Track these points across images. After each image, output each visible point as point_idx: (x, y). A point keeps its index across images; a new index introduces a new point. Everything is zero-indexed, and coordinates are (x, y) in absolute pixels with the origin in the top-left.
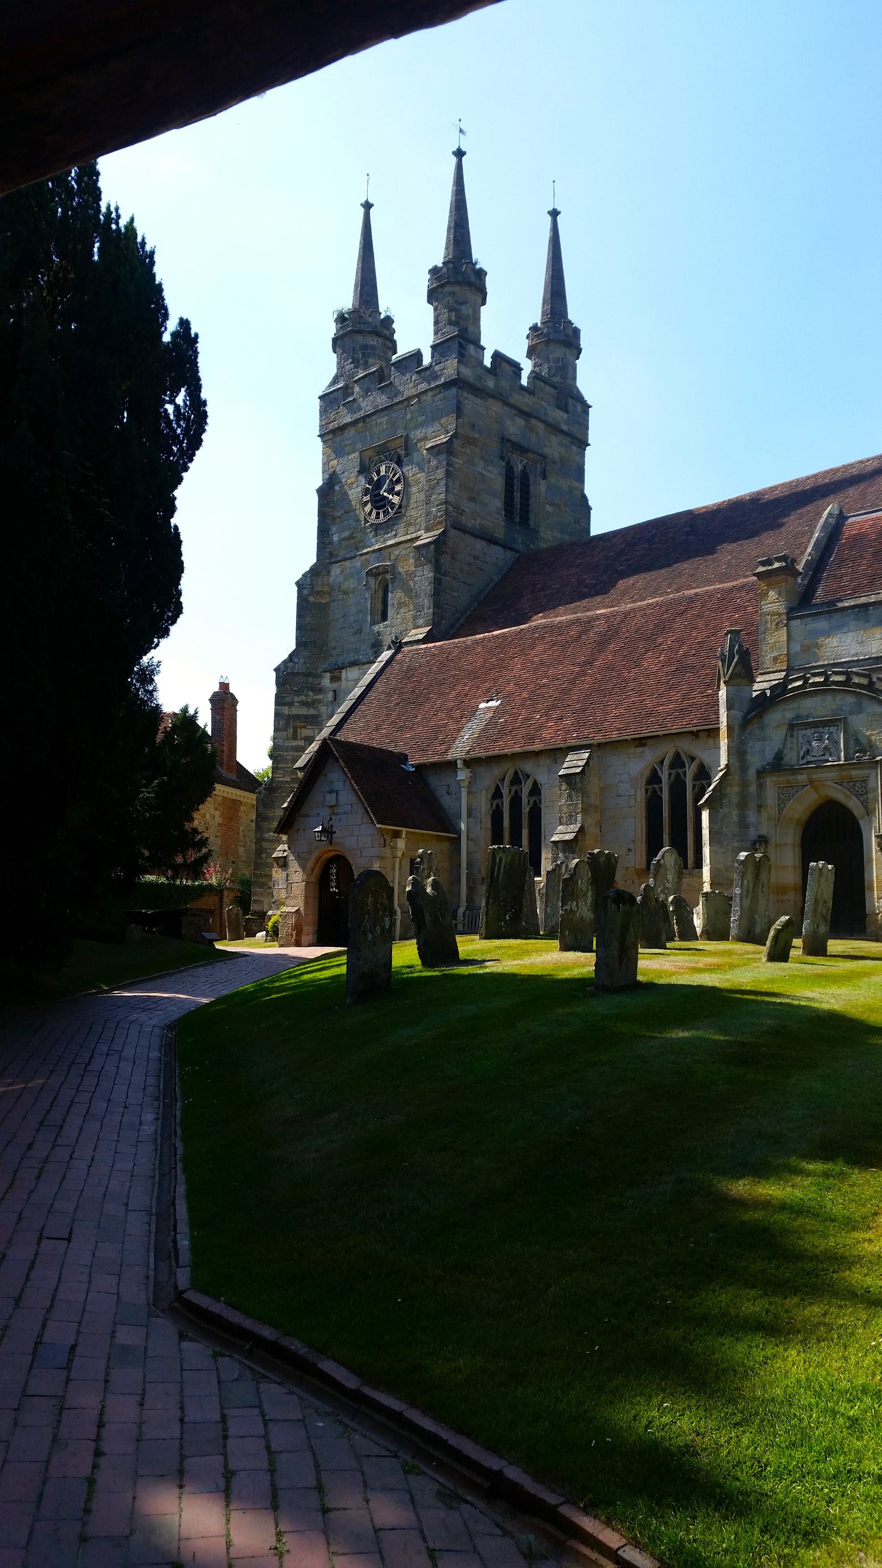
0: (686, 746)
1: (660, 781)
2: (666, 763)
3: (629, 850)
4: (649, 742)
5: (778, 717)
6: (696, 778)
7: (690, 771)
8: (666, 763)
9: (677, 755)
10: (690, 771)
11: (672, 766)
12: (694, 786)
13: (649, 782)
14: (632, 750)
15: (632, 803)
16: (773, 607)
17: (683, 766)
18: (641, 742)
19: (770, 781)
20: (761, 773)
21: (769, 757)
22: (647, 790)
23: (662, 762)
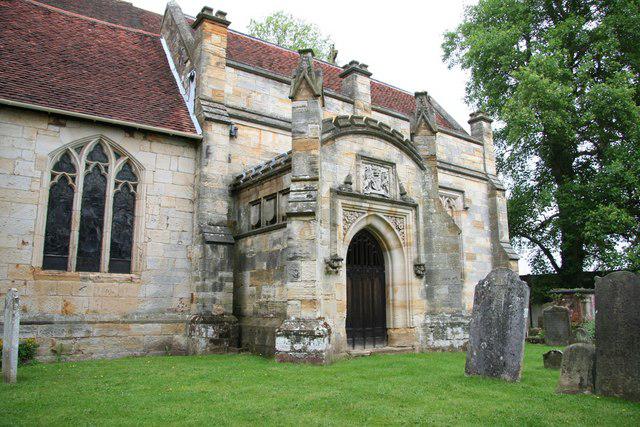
0: (119, 139)
1: (73, 168)
2: (86, 151)
3: (23, 243)
4: (69, 124)
5: (349, 145)
6: (120, 175)
7: (114, 167)
8: (86, 151)
9: (99, 146)
10: (114, 167)
11: (91, 156)
12: (117, 184)
13: (57, 167)
14: (44, 125)
15: (36, 186)
16: (216, 49)
17: (106, 158)
18: (59, 120)
19: (340, 201)
20: (337, 192)
21: (341, 180)
22: (53, 176)
23: (79, 149)
